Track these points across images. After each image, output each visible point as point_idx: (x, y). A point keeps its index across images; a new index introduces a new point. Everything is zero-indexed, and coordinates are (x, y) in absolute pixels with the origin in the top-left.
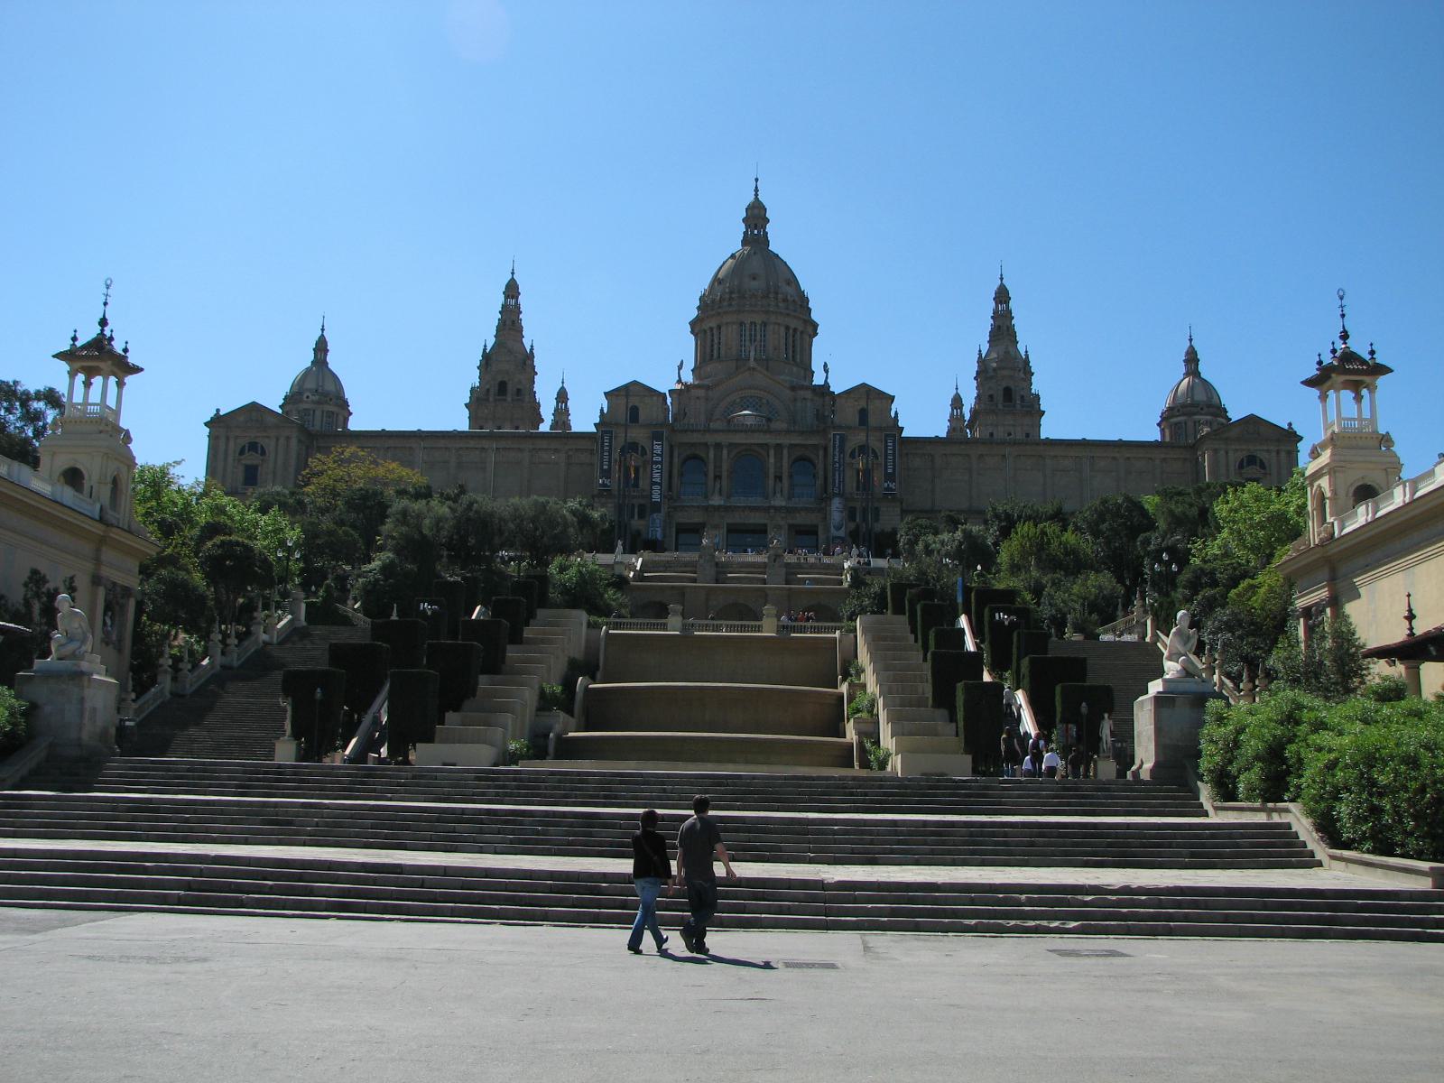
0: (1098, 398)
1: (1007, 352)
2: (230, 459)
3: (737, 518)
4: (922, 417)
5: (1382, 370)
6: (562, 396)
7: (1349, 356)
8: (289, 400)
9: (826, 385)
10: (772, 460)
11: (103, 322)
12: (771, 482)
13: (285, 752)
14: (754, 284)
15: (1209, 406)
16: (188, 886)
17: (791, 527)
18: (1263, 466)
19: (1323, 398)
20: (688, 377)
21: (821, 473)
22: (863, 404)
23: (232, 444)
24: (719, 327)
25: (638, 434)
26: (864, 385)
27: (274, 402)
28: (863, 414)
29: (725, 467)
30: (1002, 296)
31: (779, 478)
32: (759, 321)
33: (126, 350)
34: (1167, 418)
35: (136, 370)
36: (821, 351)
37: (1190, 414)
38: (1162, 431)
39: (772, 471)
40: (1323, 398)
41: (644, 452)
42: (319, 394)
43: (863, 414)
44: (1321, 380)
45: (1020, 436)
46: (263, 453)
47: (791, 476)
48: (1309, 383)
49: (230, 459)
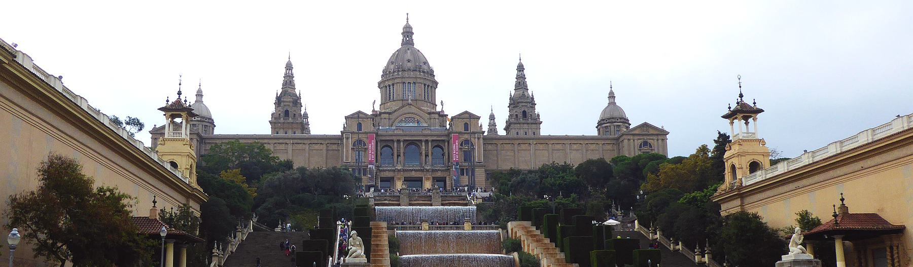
1: (524, 95)
3: (408, 175)
7: (745, 105)
14: (409, 64)
18: (651, 146)
19: (732, 123)
20: (377, 108)
26: (466, 112)
29: (402, 151)
30: (521, 68)
31: (427, 156)
34: (600, 124)
36: (440, 94)
38: (599, 130)
40: (732, 123)
41: (365, 145)
44: (731, 116)
45: (530, 135)
48: (725, 117)
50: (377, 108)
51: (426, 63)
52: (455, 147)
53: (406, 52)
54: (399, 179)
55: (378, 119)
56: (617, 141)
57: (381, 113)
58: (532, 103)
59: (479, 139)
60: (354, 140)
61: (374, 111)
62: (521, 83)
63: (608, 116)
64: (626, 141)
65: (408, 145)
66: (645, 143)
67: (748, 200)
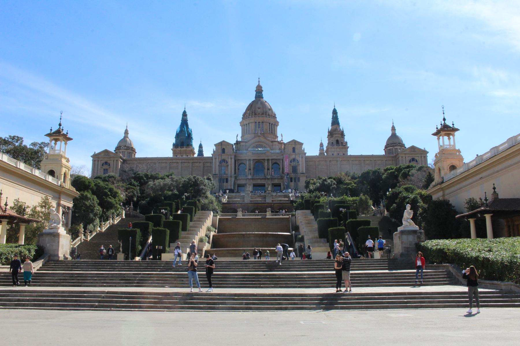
0: (366, 143)
2: (99, 167)
4: (311, 150)
5: (457, 130)
6: (201, 146)
8: (118, 148)
9: (282, 140)
10: (266, 164)
11: (60, 125)
12: (266, 170)
13: (121, 257)
14: (259, 110)
15: (399, 143)
16: (99, 302)
17: (273, 184)
18: (417, 161)
19: (439, 139)
21: (281, 168)
22: (294, 146)
23: (99, 162)
24: (249, 124)
25: (224, 157)
26: (294, 140)
27: (112, 149)
28: (294, 149)
31: (268, 169)
32: (261, 122)
33: (67, 133)
34: (386, 147)
35: (70, 139)
37: (393, 146)
38: (385, 152)
39: (266, 167)
40: (439, 139)
41: (227, 162)
42: (125, 147)
43: (294, 149)
44: (437, 134)
46: (109, 165)
47: (272, 169)
49: (99, 167)
50: (239, 139)
51: (270, 109)
52: (286, 163)
53: (257, 103)
54: (250, 185)
55: (239, 145)
56: (395, 158)
57: (240, 142)
58: (342, 134)
59: (302, 157)
60: (220, 159)
61: (237, 141)
62: (335, 121)
63: (391, 142)
64: (400, 158)
65: (256, 162)
66: (413, 160)
67: (447, 192)
